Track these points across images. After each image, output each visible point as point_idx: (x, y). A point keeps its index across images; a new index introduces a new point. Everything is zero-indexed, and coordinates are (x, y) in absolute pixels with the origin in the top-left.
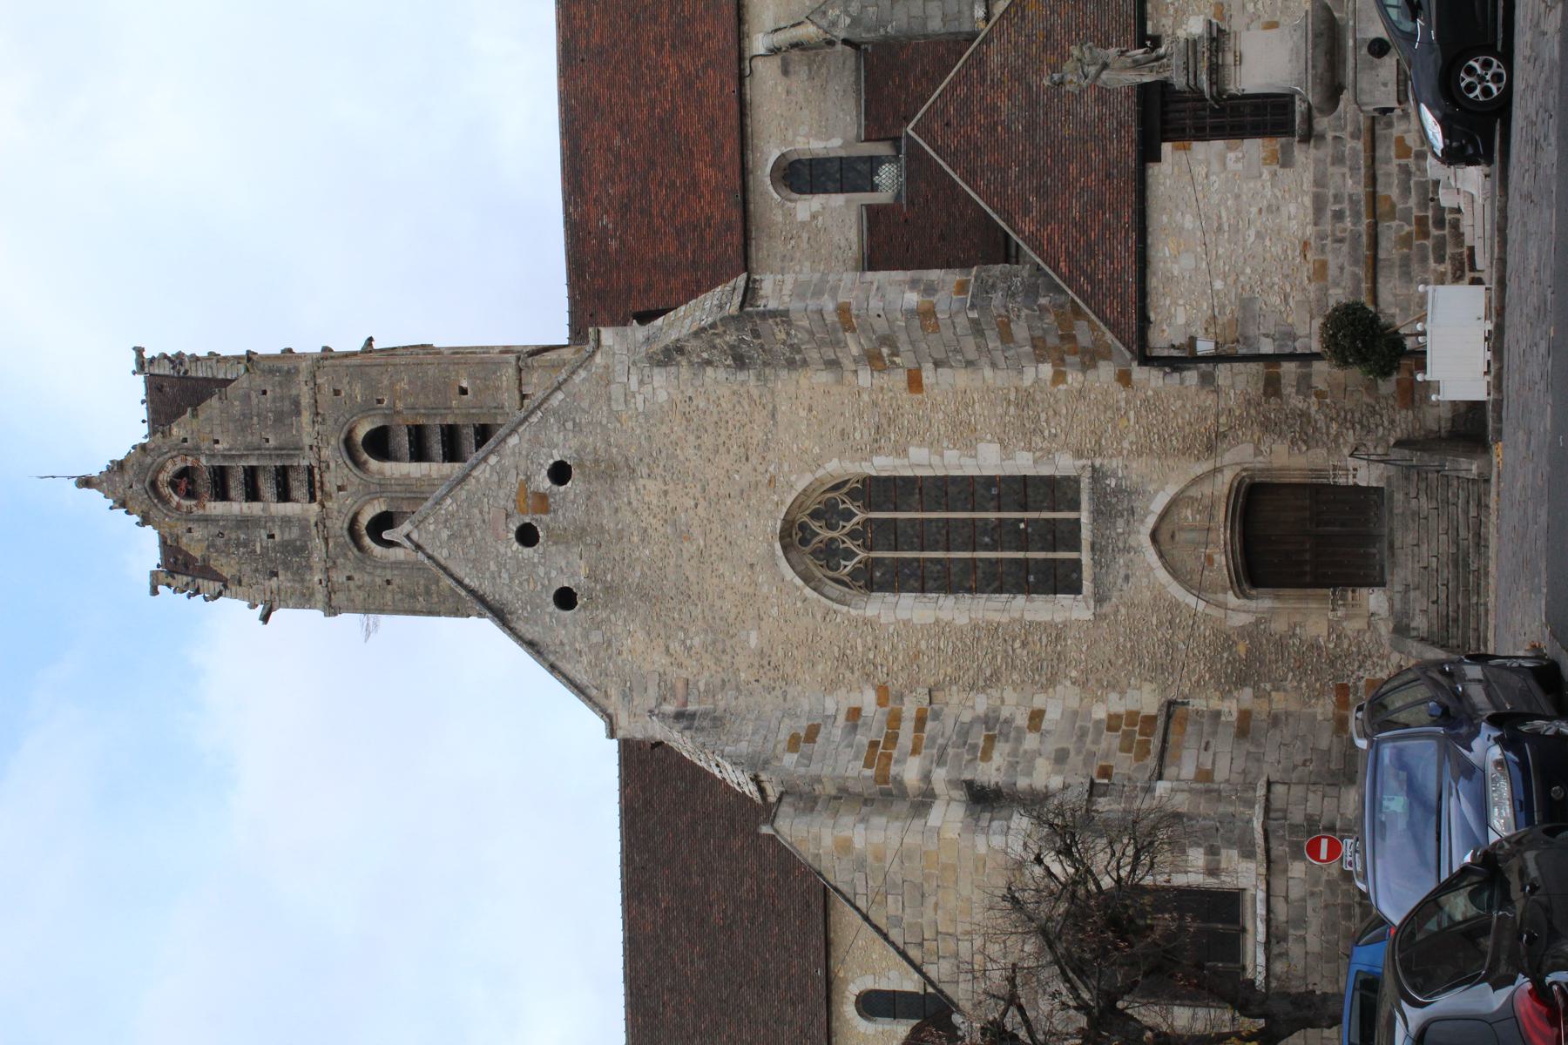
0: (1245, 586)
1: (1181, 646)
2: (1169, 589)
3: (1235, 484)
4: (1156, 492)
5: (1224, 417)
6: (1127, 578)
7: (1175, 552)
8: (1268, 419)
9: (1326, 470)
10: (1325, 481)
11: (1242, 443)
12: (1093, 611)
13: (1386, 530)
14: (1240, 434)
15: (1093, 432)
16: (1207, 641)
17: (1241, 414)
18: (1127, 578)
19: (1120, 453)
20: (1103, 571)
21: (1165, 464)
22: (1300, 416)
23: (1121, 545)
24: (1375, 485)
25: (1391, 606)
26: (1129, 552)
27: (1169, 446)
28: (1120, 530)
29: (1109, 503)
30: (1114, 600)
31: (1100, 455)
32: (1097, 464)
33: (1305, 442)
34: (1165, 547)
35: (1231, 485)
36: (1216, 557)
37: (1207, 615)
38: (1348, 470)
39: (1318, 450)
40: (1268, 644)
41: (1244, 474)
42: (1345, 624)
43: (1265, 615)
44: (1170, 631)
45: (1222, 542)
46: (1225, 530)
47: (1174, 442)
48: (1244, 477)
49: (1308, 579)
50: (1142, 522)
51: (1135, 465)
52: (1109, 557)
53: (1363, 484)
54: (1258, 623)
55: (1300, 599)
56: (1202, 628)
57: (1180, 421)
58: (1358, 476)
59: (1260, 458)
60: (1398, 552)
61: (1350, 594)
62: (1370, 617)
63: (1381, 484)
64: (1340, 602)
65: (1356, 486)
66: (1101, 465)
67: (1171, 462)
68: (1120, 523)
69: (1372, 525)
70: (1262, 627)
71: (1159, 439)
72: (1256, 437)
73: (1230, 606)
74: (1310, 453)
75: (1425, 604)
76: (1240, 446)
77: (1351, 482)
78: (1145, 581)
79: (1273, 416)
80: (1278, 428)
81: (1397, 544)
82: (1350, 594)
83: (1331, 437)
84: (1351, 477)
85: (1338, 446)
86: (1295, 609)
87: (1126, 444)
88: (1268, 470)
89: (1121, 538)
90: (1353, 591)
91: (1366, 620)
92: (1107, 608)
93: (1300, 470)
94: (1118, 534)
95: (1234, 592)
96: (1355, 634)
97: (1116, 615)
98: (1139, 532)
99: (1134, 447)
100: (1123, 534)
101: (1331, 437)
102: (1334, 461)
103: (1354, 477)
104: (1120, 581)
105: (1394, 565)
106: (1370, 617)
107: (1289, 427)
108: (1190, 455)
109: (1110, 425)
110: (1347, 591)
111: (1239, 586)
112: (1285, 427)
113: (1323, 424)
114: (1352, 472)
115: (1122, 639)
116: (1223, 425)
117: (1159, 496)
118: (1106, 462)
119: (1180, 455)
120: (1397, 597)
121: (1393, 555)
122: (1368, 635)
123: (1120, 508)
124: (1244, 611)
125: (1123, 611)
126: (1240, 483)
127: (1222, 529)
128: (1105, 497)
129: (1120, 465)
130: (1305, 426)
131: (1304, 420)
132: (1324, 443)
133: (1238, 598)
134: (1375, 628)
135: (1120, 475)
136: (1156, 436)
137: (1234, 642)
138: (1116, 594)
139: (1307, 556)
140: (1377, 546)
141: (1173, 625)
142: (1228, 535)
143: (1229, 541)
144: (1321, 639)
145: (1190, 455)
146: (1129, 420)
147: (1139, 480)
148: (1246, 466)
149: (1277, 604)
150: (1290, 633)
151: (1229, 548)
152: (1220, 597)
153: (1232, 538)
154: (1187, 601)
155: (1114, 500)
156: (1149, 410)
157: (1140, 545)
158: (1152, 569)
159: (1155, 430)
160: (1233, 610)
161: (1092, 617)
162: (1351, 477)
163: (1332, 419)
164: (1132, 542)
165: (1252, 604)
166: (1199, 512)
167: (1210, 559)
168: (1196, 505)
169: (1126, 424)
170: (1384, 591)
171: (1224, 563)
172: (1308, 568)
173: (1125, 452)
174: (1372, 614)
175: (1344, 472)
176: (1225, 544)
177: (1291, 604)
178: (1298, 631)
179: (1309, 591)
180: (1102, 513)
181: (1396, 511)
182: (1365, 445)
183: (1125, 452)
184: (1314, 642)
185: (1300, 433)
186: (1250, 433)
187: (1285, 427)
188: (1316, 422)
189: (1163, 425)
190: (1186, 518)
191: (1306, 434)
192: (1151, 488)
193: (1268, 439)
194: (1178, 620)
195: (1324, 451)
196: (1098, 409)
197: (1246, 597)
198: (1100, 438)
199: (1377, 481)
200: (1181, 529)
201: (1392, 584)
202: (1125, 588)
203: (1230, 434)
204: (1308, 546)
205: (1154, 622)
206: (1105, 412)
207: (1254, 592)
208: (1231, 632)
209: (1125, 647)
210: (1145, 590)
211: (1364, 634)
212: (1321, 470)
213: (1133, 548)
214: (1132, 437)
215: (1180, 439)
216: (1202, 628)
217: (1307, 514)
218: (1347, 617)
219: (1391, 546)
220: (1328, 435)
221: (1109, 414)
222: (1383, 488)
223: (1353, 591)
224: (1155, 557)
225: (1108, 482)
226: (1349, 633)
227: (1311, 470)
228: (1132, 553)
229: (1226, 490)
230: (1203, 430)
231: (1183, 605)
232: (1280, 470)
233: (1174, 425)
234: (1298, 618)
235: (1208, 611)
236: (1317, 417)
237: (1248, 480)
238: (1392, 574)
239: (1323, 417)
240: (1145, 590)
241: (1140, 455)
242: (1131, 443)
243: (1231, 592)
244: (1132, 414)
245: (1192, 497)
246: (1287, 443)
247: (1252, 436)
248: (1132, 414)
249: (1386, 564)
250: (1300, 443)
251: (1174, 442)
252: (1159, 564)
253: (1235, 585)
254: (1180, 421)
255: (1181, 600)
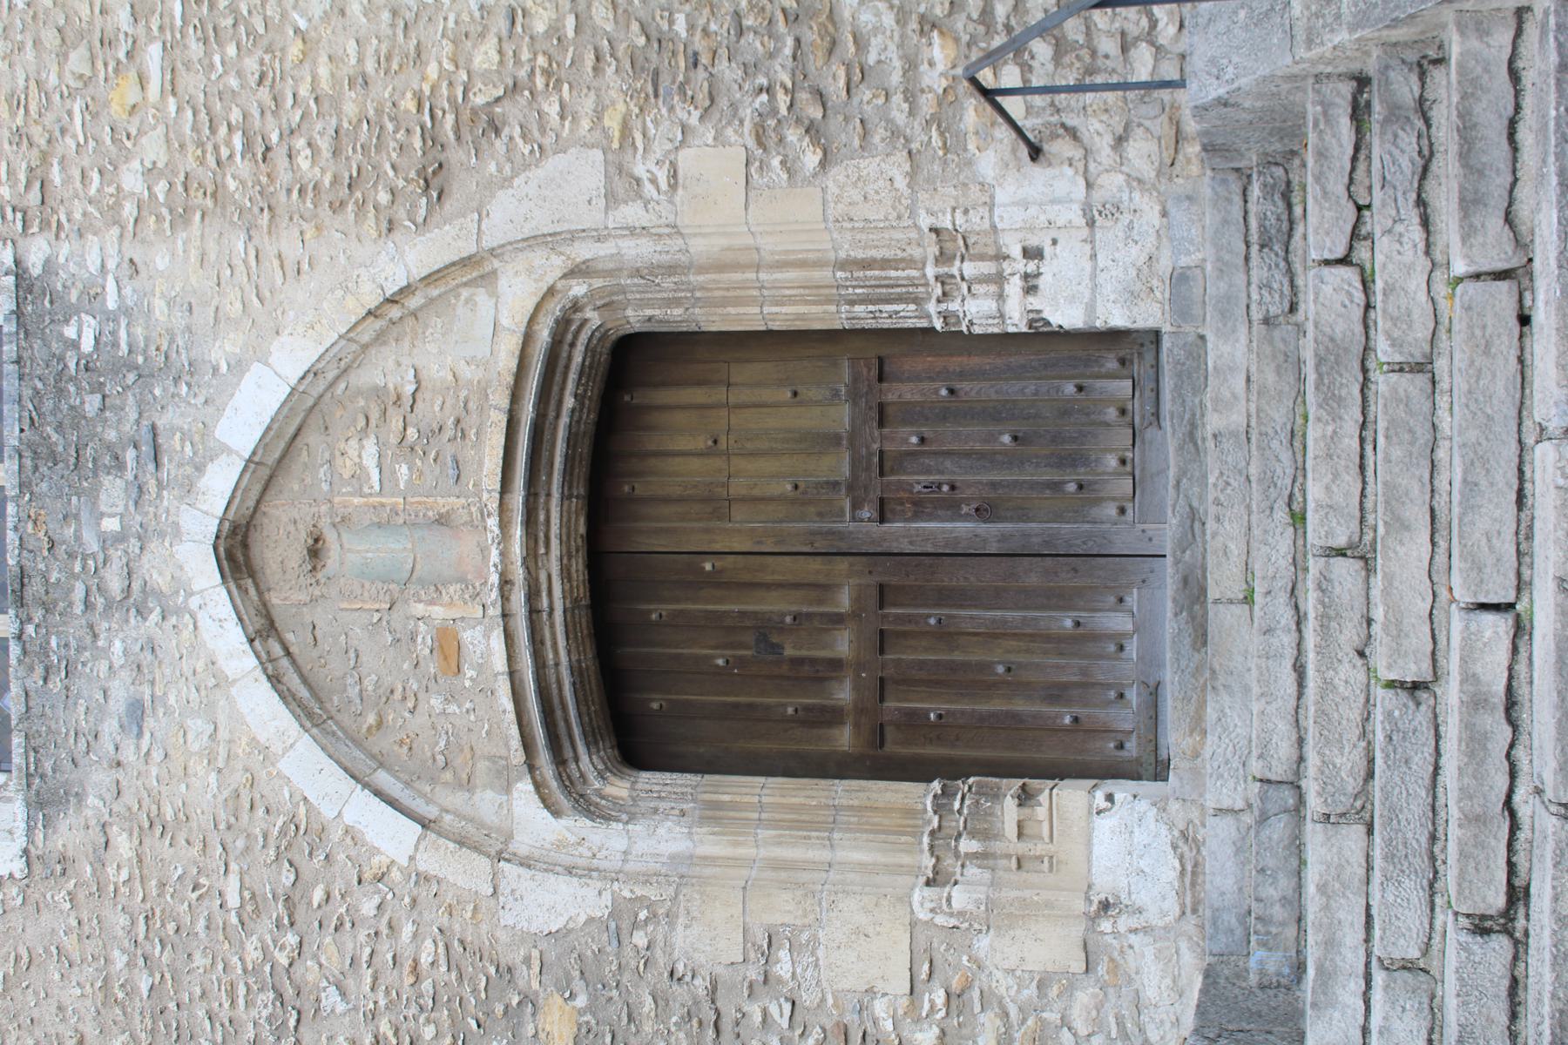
0: (587, 763)
1: (331, 998)
2: (285, 766)
3: (544, 335)
4: (238, 367)
5: (490, 45)
6: (136, 714)
7: (321, 616)
8: (660, 41)
9: (910, 263)
10: (906, 316)
11: (560, 147)
12: (21, 842)
13: (1168, 533)
14: (552, 109)
15: (19, 136)
16: (426, 986)
17: (555, 30)
18: (136, 714)
19: (112, 215)
20: (56, 684)
21: (270, 250)
22: (792, 18)
23: (115, 585)
24: (1118, 320)
25: (1192, 874)
26: (142, 613)
27: (284, 177)
28: (111, 525)
29: (77, 412)
30: (92, 800)
31: (45, 225)
32: (35, 268)
33: (811, 130)
34: (286, 595)
35: (528, 338)
36: (470, 636)
37: (424, 878)
38: (1001, 257)
39: (869, 166)
40: (660, 1016)
41: (578, 289)
42: (983, 944)
43: (652, 893)
44: (291, 939)
45: (494, 579)
46: (504, 525)
47: (303, 163)
48: (576, 306)
49: (844, 738)
50: (188, 489)
51: (161, 262)
52: (75, 630)
53: (1067, 316)
54: (620, 922)
55: (801, 824)
56: (407, 930)
57: (323, 71)
58: (1042, 282)
59: (632, 213)
60: (1225, 619)
61: (1009, 810)
62: (1093, 919)
63: (1147, 315)
64: (967, 845)
65: (1042, 336)
66: (49, 265)
67: (289, 244)
68: (113, 491)
69: (1111, 510)
70: (640, 939)
71: (248, 146)
72: (612, 122)
73: (522, 844)
74: (837, 173)
75: (1413, 919)
76: (554, 163)
77: (1017, 322)
78: (198, 725)
79: (681, 26)
80: (701, 74)
81: (1223, 580)
82: (1009, 810)
83: (927, 104)
84: (1014, 287)
85: (953, 143)
86: (778, 865)
87: (131, 180)
88: (672, 269)
89: (116, 554)
90: (1025, 797)
91: (1077, 931)
92: (69, 834)
93: (802, 264)
94: (105, 541)
95: (538, 786)
96: (1031, 992)
97: (99, 863)
98: (176, 528)
99: (161, 188)
100: (120, 538)
101: (927, 104)
102: (937, 210)
103: (1030, 289)
104: (110, 727)
105: (1205, 680)
106: (1093, 919)
107: (749, 70)
108: (361, 207)
109: (77, 108)
110: (996, 796)
111: (559, 761)
112: (728, 72)
113: (893, 53)
114: (1021, 265)
115: (120, 960)
116: (486, 76)
117: (248, 381)
118: (65, 249)
119: (325, 212)
120: (1219, 836)
121: (1201, 638)
122: (1084, 997)
123: (111, 435)
124: (570, 871)
125: (124, 845)
126: (562, 324)
127: (492, 522)
128: (61, 393)
129: (111, 264)
130: (815, 62)
131: (810, 36)
132: (895, 133)
133: (556, 813)
134: (1114, 967)
135: (111, 303)
136: (237, 141)
137: (528, 999)
138: (99, 779)
139: (843, 644)
140: (1132, 599)
141: (300, 916)
142: (517, 549)
143: (518, 574)
144: (880, 1008)
145: (361, 207)
146: (142, 81)
147: (179, 320)
148: (584, 251)
149: (711, 844)
150: (754, 974)
151: (518, 598)
152: (486, 802)
153: (531, 558)
154: (349, 818)
155: (92, 403)
156: (212, 36)
157: (181, 585)
158: (222, 682)
159: (235, 116)
160: (526, 863)
161: (18, 867)
162: (1014, 287)
163: (928, 25)
164: (154, 571)
165: (609, 840)
166: (406, 449)
167: (448, 648)
168: (396, 423)
169: (133, 95)
170: (1161, 805)
171: (500, 662)
172: (843, 693)
173: (129, 210)
174: (1105, 906)
175: (987, 268)
176: (505, 583)
177: (765, 846)
178: (783, 968)
179: (844, 791)
180: (54, 459)
181: (1213, 422)
182: (1073, 133)
183: (129, 210)
184: (850, 1018)
185: (791, 92)
186: (587, 104)
187: (728, 72)
188: (860, 42)
189: (264, 94)
190: (359, 476)
191: (820, 96)
192: (220, 352)
193: (661, 128)
194: (318, 895)
195: (897, 168)
196: (37, 43)
197: (588, 807)
198: (45, 157)
199: (1133, 296)
200: (343, 522)
201: (1197, 774)
202: (129, 755)
203: (513, 112)
204: (844, 601)
205: (233, 901)
206: (62, 57)
207: (618, 788)
208: (515, 957)
209: (130, 989)
210: (199, 767)
211: (1069, 990)
212: (885, 264)
213: (159, 595)
214: (153, 149)
215: (324, 144)
216: (407, 930)
217: (839, 465)
218: (993, 916)
219: (1194, 591)
220: (910, 97)
221: (77, 61)
222: (1156, 335)
223: (1025, 797)
224: (234, 636)
225: (70, 332)
226: (1004, 985)
227: (844, 265)
228: (155, 617)
229: (506, 362)
230: (409, 104)
231: (336, 834)
232: (721, 267)
233: (304, 91)
234: (781, 909)
235: (426, 863)
236: (866, 18)
237: (594, 318)
238: (1197, 725)
239: (889, 20)
240: (199, 767)
241: (181, 218)
242: (150, 172)
243: (525, 786)
244: (153, 55)
245: (378, 393)
246: (741, 138)
247: (598, 115)
248: (153, 55)
249: (1170, 677)
250: (793, 135)
251: (303, 163)
252: (246, 662)
253: (544, 758)
254: (323, 71)
255: (328, 812)
